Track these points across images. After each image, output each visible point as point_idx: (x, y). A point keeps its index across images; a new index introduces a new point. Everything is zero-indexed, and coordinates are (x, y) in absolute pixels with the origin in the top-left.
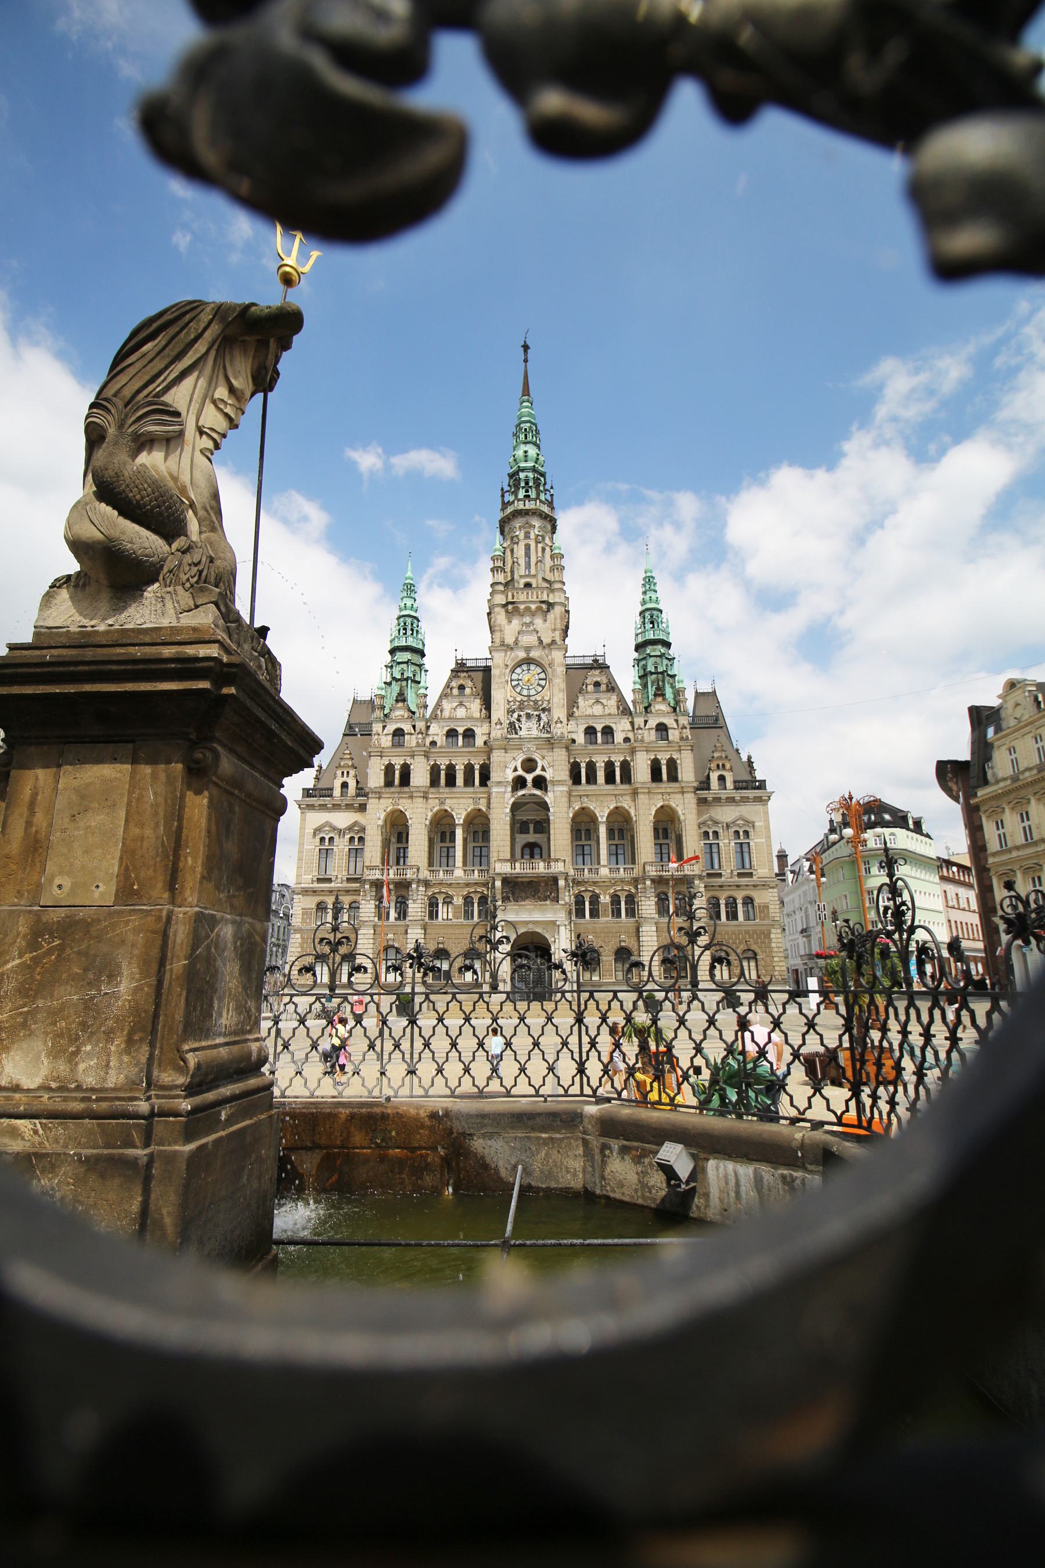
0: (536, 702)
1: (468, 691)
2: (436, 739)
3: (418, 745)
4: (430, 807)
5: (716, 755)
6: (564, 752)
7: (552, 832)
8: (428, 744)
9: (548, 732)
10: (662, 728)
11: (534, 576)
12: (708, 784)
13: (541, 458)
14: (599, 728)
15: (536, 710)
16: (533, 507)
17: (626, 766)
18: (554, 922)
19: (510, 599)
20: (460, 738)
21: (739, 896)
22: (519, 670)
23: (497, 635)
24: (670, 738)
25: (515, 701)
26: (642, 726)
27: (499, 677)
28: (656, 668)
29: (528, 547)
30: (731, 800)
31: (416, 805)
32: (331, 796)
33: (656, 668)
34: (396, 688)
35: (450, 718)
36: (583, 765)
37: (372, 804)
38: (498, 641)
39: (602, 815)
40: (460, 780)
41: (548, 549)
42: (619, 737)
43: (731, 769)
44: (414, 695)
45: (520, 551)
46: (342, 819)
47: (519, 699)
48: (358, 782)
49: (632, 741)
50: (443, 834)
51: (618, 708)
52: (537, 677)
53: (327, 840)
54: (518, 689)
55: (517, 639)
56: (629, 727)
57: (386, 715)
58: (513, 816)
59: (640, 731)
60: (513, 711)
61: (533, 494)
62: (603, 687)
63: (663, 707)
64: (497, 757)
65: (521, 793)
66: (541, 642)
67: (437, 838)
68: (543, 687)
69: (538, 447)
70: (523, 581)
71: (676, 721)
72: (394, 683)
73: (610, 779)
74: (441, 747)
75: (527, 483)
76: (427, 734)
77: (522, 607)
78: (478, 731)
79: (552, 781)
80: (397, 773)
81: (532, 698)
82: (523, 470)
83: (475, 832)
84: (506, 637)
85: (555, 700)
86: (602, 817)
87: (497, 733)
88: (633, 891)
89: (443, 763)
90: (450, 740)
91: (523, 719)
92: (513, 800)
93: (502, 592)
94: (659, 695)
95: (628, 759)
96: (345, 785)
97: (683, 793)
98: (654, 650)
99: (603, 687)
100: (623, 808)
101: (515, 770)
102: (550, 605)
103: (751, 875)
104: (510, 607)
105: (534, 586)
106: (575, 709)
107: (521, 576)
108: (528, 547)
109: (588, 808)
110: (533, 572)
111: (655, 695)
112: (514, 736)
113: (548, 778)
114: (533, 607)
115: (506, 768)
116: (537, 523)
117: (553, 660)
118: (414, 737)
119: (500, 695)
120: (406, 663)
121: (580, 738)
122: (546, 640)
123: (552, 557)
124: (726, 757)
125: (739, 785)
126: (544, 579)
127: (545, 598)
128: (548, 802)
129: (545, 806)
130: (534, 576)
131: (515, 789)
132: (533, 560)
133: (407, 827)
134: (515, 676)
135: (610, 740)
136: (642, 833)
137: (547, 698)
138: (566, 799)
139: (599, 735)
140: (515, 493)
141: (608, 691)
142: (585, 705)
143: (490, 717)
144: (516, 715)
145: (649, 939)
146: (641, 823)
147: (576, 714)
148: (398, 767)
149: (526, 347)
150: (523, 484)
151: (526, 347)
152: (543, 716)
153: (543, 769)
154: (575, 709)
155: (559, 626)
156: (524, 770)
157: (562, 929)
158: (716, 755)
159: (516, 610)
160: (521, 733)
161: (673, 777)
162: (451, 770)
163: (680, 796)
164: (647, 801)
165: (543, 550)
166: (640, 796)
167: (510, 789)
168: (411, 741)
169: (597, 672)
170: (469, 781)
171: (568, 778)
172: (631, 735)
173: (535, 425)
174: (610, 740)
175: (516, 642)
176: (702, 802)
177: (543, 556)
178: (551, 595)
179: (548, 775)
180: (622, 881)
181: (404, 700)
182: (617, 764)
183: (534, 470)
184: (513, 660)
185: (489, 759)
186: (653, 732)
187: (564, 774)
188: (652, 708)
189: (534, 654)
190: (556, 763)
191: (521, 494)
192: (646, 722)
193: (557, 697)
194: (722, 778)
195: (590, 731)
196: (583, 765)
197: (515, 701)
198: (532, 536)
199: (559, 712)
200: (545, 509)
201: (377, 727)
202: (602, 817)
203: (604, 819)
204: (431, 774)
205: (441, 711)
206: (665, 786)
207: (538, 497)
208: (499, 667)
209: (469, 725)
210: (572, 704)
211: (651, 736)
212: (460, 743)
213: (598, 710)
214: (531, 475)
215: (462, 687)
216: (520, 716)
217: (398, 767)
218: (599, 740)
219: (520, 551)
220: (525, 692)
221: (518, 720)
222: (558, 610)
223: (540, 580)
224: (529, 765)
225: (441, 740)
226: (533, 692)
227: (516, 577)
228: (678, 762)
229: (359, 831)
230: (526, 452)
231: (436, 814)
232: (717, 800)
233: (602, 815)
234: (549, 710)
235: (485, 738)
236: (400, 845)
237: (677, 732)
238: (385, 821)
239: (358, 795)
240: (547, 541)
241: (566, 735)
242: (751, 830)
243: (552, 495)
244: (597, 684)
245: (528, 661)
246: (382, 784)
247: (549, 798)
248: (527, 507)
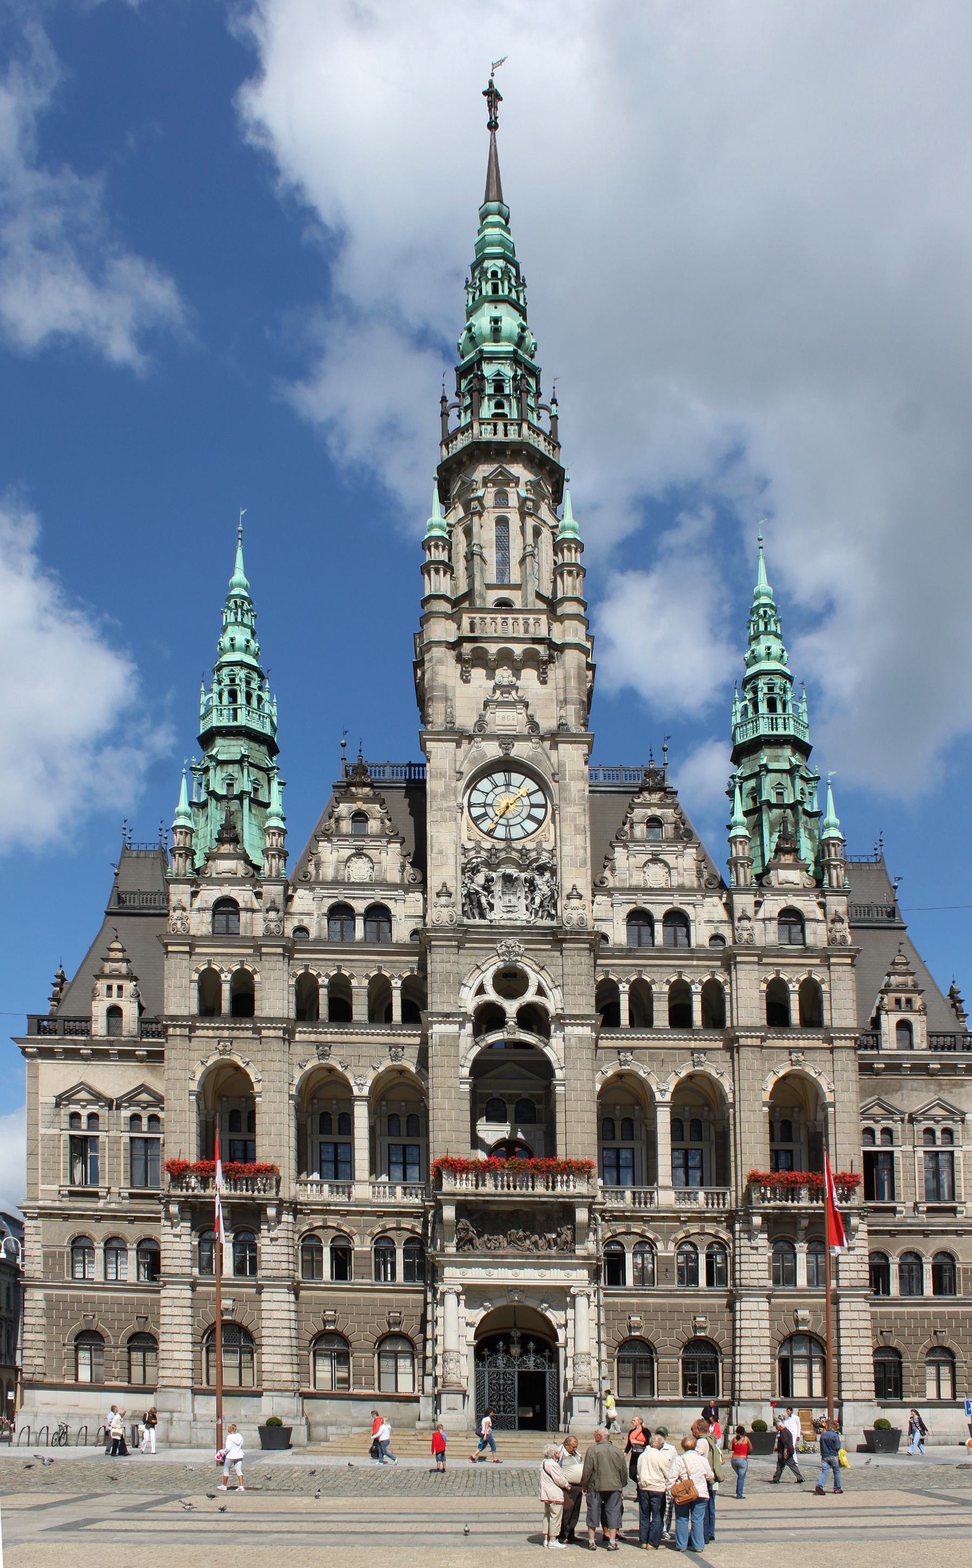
0: (524, 852)
1: (373, 826)
2: (306, 922)
3: (268, 934)
4: (297, 1059)
5: (895, 980)
6: (586, 959)
7: (560, 1117)
8: (289, 932)
9: (552, 917)
11: (517, 587)
12: (877, 1037)
13: (530, 340)
14: (658, 912)
15: (522, 868)
16: (513, 436)
17: (715, 997)
18: (563, 1291)
19: (466, 632)
20: (359, 923)
21: (928, 1249)
22: (485, 785)
25: (478, 848)
27: (444, 796)
29: (502, 522)
30: (921, 1069)
31: (269, 1055)
32: (87, 1032)
34: (217, 815)
35: (336, 883)
36: (624, 988)
37: (175, 1050)
39: (663, 1088)
40: (360, 1010)
41: (546, 533)
43: (923, 1011)
44: (255, 830)
45: (486, 531)
46: (113, 1079)
47: (487, 845)
48: (141, 1009)
50: (325, 1119)
51: (699, 874)
52: (526, 801)
53: (84, 1119)
54: (486, 825)
55: (481, 718)
57: (198, 871)
58: (473, 1092)
59: (745, 923)
60: (475, 870)
61: (511, 410)
62: (668, 830)
64: (440, 962)
65: (493, 1038)
66: (534, 725)
67: (313, 1125)
68: (540, 823)
69: (522, 312)
70: (493, 596)
72: (212, 803)
73: (680, 1017)
74: (318, 941)
75: (499, 387)
76: (287, 913)
77: (493, 648)
78: (396, 909)
79: (559, 1017)
80: (226, 989)
81: (517, 845)
82: (493, 358)
83: (392, 1117)
84: (457, 713)
85: (567, 850)
86: (663, 1092)
87: (442, 914)
88: (724, 1235)
89: (323, 975)
90: (337, 926)
91: (497, 888)
92: (477, 1049)
93: (448, 616)
96: (114, 1012)
100: (706, 1077)
101: (481, 990)
102: (556, 649)
103: (953, 1210)
104: (467, 648)
105: (518, 605)
106: (607, 873)
107: (489, 587)
108: (502, 522)
109: (633, 1075)
110: (515, 578)
112: (478, 921)
113: (552, 1011)
114: (518, 649)
115: (463, 985)
117: (561, 765)
118: (259, 916)
119: (447, 837)
120: (240, 762)
121: (618, 934)
122: (547, 723)
123: (558, 547)
124: (915, 985)
125: (937, 1040)
126: (539, 596)
128: (552, 1056)
129: (545, 1069)
130: (517, 587)
131: (478, 1032)
132: (515, 553)
133: (250, 1099)
134: (477, 797)
135: (682, 939)
136: (745, 1127)
137: (548, 846)
138: (587, 1054)
140: (473, 409)
142: (628, 865)
143: (424, 881)
144: (480, 878)
145: (755, 1324)
146: (745, 1106)
147: (610, 883)
148: (226, 977)
150: (489, 390)
152: (539, 881)
153: (541, 991)
154: (607, 873)
155: (574, 695)
156: (499, 991)
157: (581, 1302)
160: (491, 916)
162: (340, 988)
164: (756, 1065)
165: (537, 533)
167: (469, 1027)
168: (254, 924)
170: (379, 1012)
171: (592, 1011)
173: (516, 266)
174: (682, 939)
175: (481, 723)
176: (865, 1068)
177: (536, 545)
179: (553, 1003)
180: (700, 1217)
181: (236, 840)
182: (697, 988)
183: (515, 359)
184: (473, 761)
185: (423, 966)
187: (586, 1005)
189: (521, 750)
190: (568, 980)
191: (487, 409)
193: (572, 849)
194: (904, 1026)
195: (639, 918)
196: (624, 988)
197: (478, 848)
198: (513, 501)
199: (575, 877)
200: (542, 445)
201: (179, 893)
202: (663, 1092)
203: (668, 1097)
204: (298, 994)
205: (318, 866)
207: (522, 419)
208: (442, 775)
209: (378, 896)
210: (602, 861)
212: (359, 933)
213: (656, 876)
214: (508, 371)
215: (360, 817)
216: (489, 880)
217: (226, 977)
218: (659, 939)
219: (486, 531)
220: (500, 832)
221: (487, 888)
222: (572, 658)
223: (531, 597)
224: (511, 981)
225: (317, 926)
226: (516, 832)
227: (478, 586)
229: (150, 1105)
230: (496, 320)
231: (308, 1078)
232: (894, 1068)
233: (663, 1088)
234: (554, 873)
235: (413, 924)
236: (235, 1136)
238: (203, 1085)
239: (144, 1033)
240: (544, 512)
241: (590, 923)
243: (554, 418)
244: (654, 822)
245: (507, 765)
246: (195, 1010)
247: (554, 1050)
248: (500, 437)
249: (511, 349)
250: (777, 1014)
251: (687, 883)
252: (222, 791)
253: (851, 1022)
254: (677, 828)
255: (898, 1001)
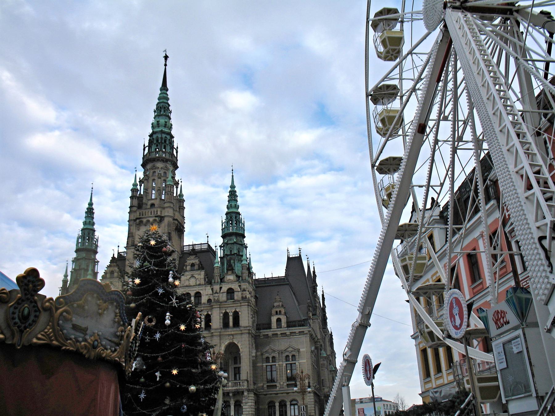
1: (116, 274)
10: (230, 292)
14: (193, 294)
23: (131, 239)
24: (236, 298)
26: (218, 291)
28: (231, 251)
33: (231, 251)
38: (130, 243)
42: (204, 299)
49: (213, 301)
51: (205, 280)
56: (210, 292)
59: (216, 295)
62: (196, 267)
63: (231, 277)
70: (150, 202)
71: (240, 286)
75: (157, 141)
94: (230, 270)
95: (210, 313)
97: (242, 334)
98: (230, 240)
99: (196, 267)
104: (138, 221)
111: (228, 270)
114: (151, 220)
116: (160, 165)
124: (282, 306)
127: (159, 213)
139: (193, 299)
141: (199, 269)
149: (166, 57)
150: (155, 142)
151: (166, 57)
158: (276, 304)
159: (141, 222)
161: (236, 323)
163: (239, 336)
166: (215, 338)
169: (192, 257)
172: (211, 298)
178: (163, 211)
186: (225, 295)
188: (225, 280)
192: (221, 288)
206: (231, 331)
211: (223, 297)
213: (192, 282)
228: (240, 313)
237: (240, 293)
242: (296, 354)
244: (193, 265)
249: (160, 129)
250: (226, 325)
251: (201, 283)
252: (77, 268)
253: (247, 325)
254: (199, 266)
255: (277, 312)
